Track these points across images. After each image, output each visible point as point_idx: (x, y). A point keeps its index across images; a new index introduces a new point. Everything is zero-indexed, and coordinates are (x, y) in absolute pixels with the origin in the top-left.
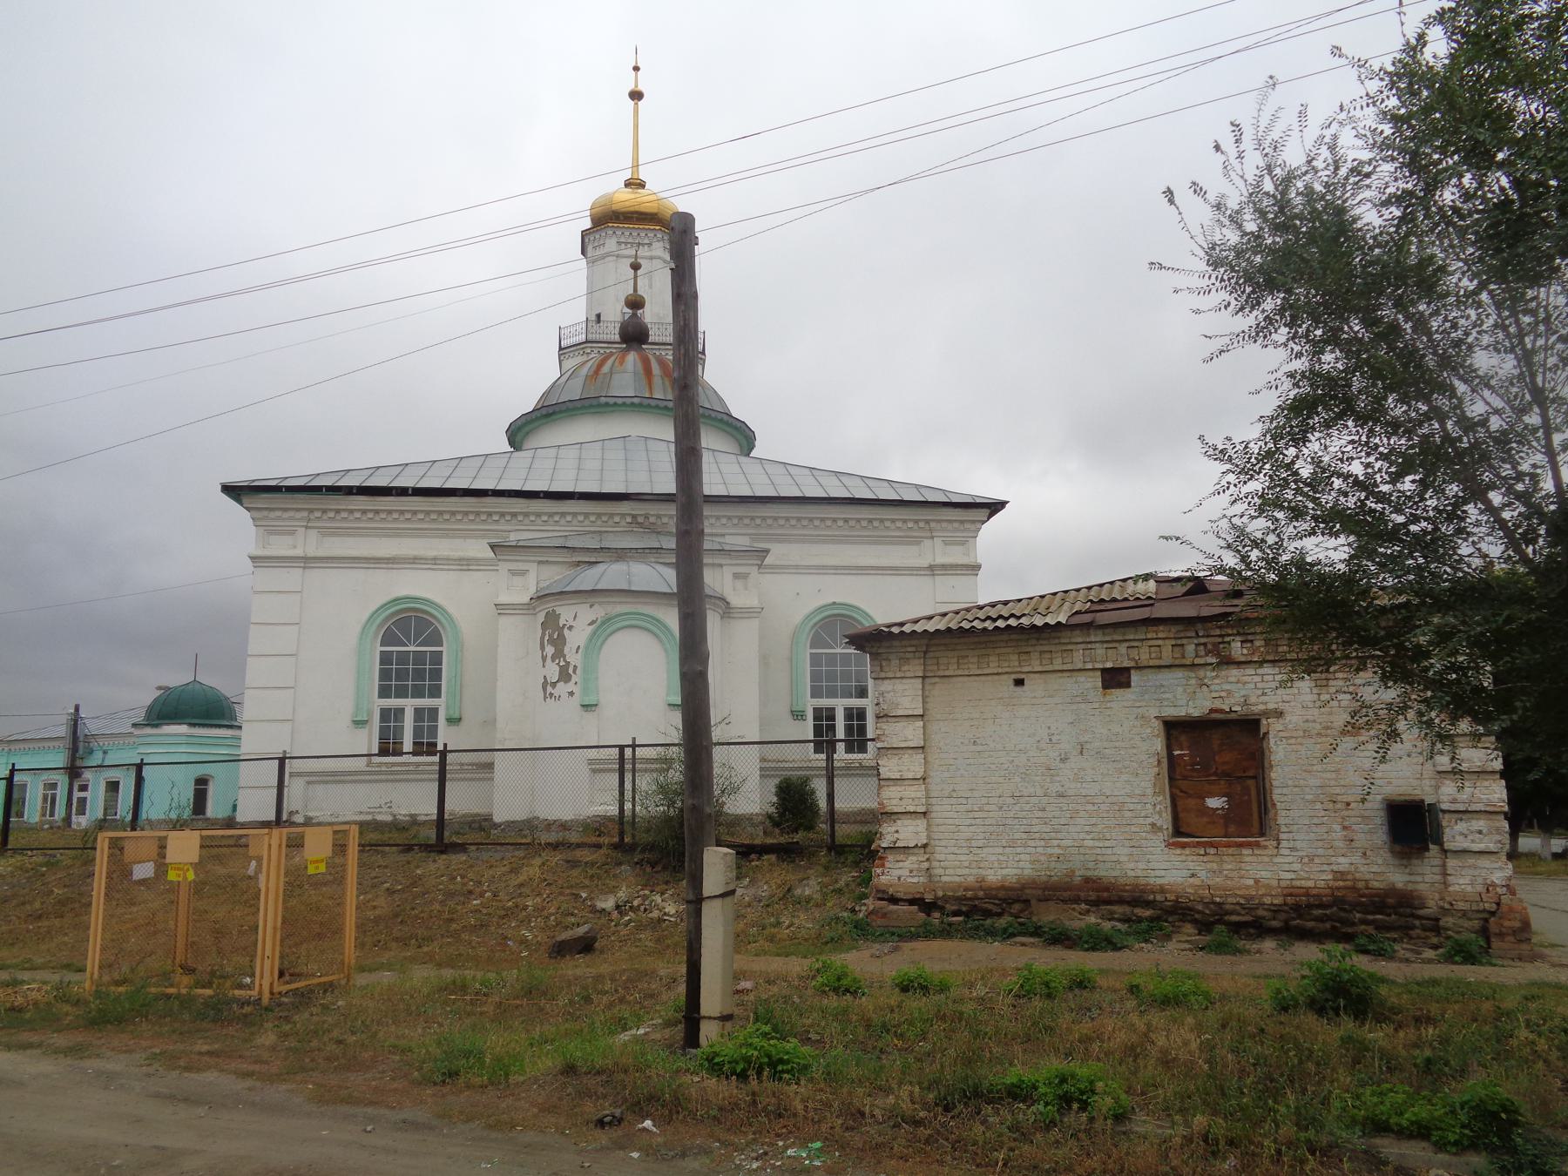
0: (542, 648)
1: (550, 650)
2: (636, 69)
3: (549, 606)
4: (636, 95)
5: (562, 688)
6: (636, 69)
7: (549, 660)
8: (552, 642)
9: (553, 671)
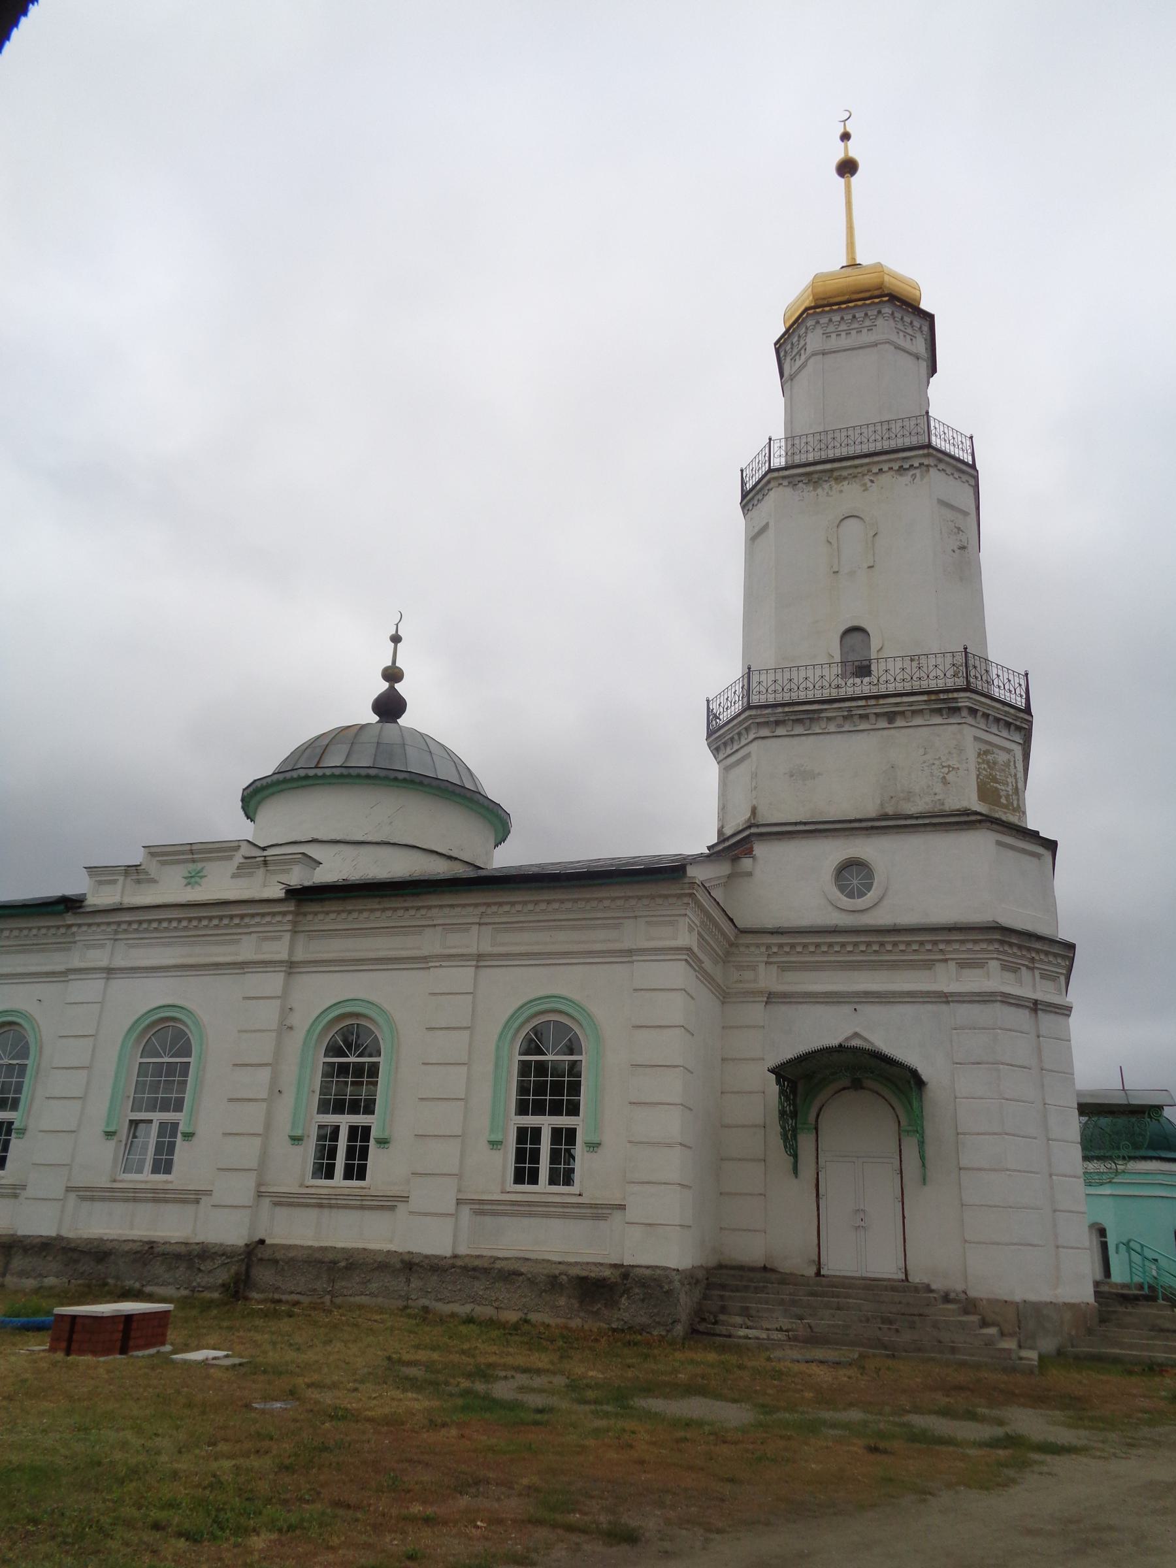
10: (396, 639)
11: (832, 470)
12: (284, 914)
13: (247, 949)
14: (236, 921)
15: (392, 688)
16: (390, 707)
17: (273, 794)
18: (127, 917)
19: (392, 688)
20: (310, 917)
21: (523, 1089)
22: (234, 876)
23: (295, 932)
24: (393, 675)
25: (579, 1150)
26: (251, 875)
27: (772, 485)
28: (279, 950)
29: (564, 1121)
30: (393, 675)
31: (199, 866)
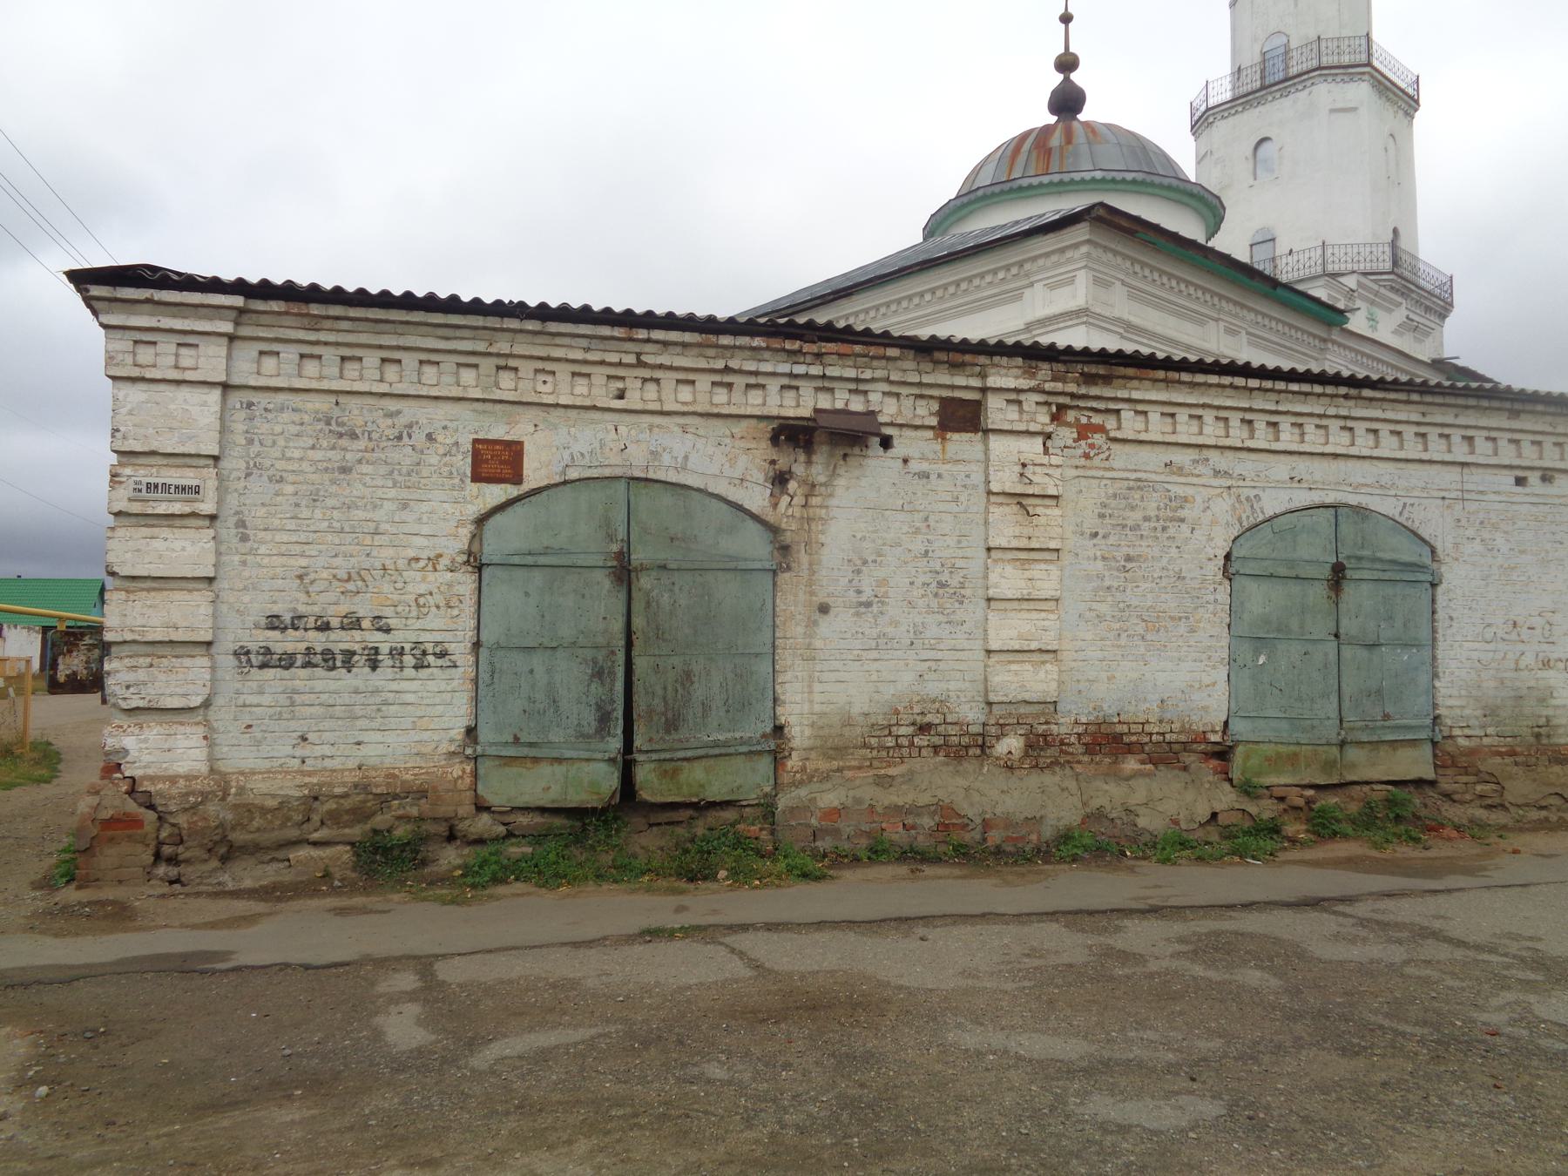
10: (1066, 19)
11: (1387, 89)
15: (1067, 80)
16: (1067, 102)
17: (1187, 205)
18: (1367, 349)
19: (1067, 80)
24: (1067, 63)
26: (1401, 334)
27: (1366, 77)
30: (1067, 63)
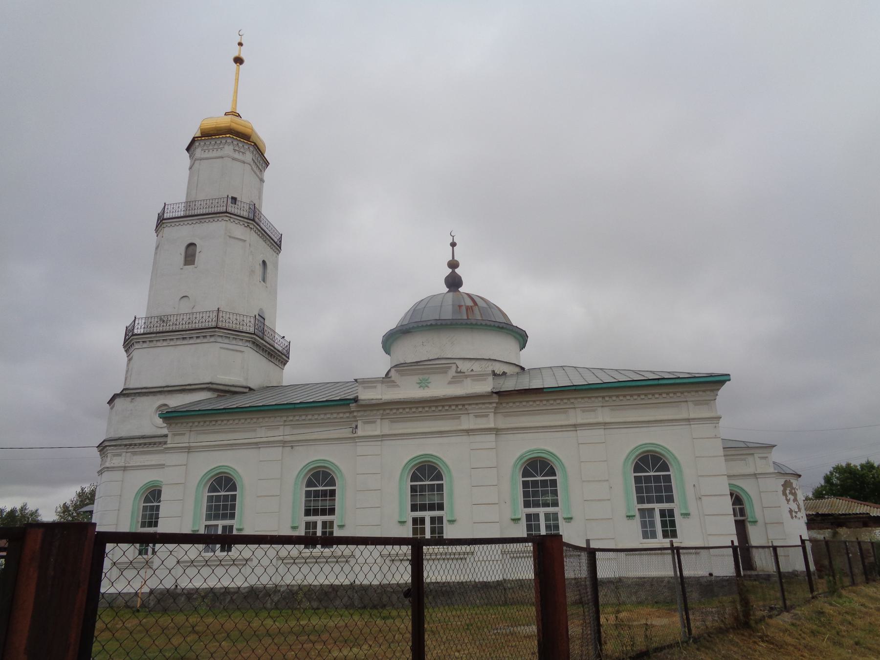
0: (784, 494)
1: (791, 497)
2: (240, 44)
3: (788, 478)
4: (239, 60)
5: (799, 515)
6: (240, 44)
7: (791, 501)
8: (791, 493)
9: (794, 507)
12: (491, 403)
13: (468, 422)
14: (460, 407)
20: (504, 405)
21: (639, 490)
22: (450, 383)
23: (495, 413)
25: (678, 518)
28: (490, 422)
29: (665, 506)
31: (426, 376)
